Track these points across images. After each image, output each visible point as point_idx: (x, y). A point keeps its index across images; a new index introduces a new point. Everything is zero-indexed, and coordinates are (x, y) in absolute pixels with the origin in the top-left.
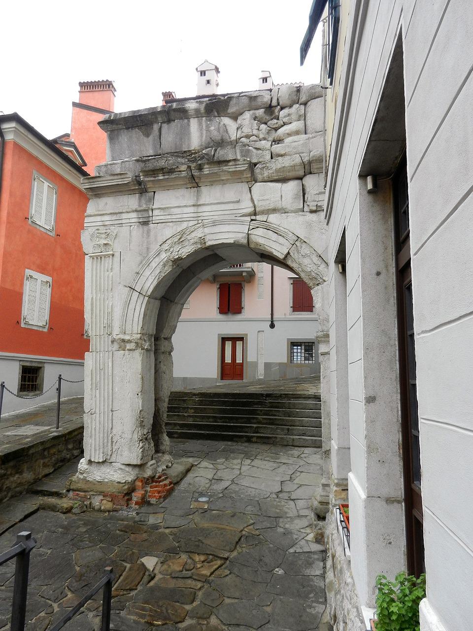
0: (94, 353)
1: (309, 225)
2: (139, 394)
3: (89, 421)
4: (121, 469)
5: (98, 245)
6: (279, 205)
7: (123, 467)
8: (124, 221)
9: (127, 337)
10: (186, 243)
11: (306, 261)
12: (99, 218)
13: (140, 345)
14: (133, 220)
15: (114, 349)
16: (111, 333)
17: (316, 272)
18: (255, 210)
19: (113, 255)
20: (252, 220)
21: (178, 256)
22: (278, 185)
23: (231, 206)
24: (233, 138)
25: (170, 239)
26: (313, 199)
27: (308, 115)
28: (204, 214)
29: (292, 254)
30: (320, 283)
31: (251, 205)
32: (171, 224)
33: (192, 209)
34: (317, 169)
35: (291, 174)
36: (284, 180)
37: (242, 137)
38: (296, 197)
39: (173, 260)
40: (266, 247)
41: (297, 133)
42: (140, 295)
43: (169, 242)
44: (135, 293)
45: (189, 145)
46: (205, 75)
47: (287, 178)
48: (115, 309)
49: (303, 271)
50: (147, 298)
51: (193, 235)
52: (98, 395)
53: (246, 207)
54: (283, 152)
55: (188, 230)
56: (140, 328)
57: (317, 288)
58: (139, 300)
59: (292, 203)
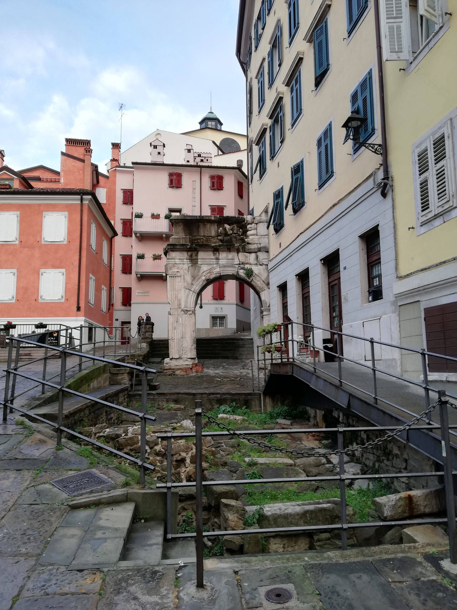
3: (171, 343)
9: (189, 309)
11: (258, 283)
23: (230, 261)
27: (258, 228)
33: (215, 260)
41: (254, 235)
46: (156, 148)
48: (182, 298)
51: (215, 270)
53: (236, 262)
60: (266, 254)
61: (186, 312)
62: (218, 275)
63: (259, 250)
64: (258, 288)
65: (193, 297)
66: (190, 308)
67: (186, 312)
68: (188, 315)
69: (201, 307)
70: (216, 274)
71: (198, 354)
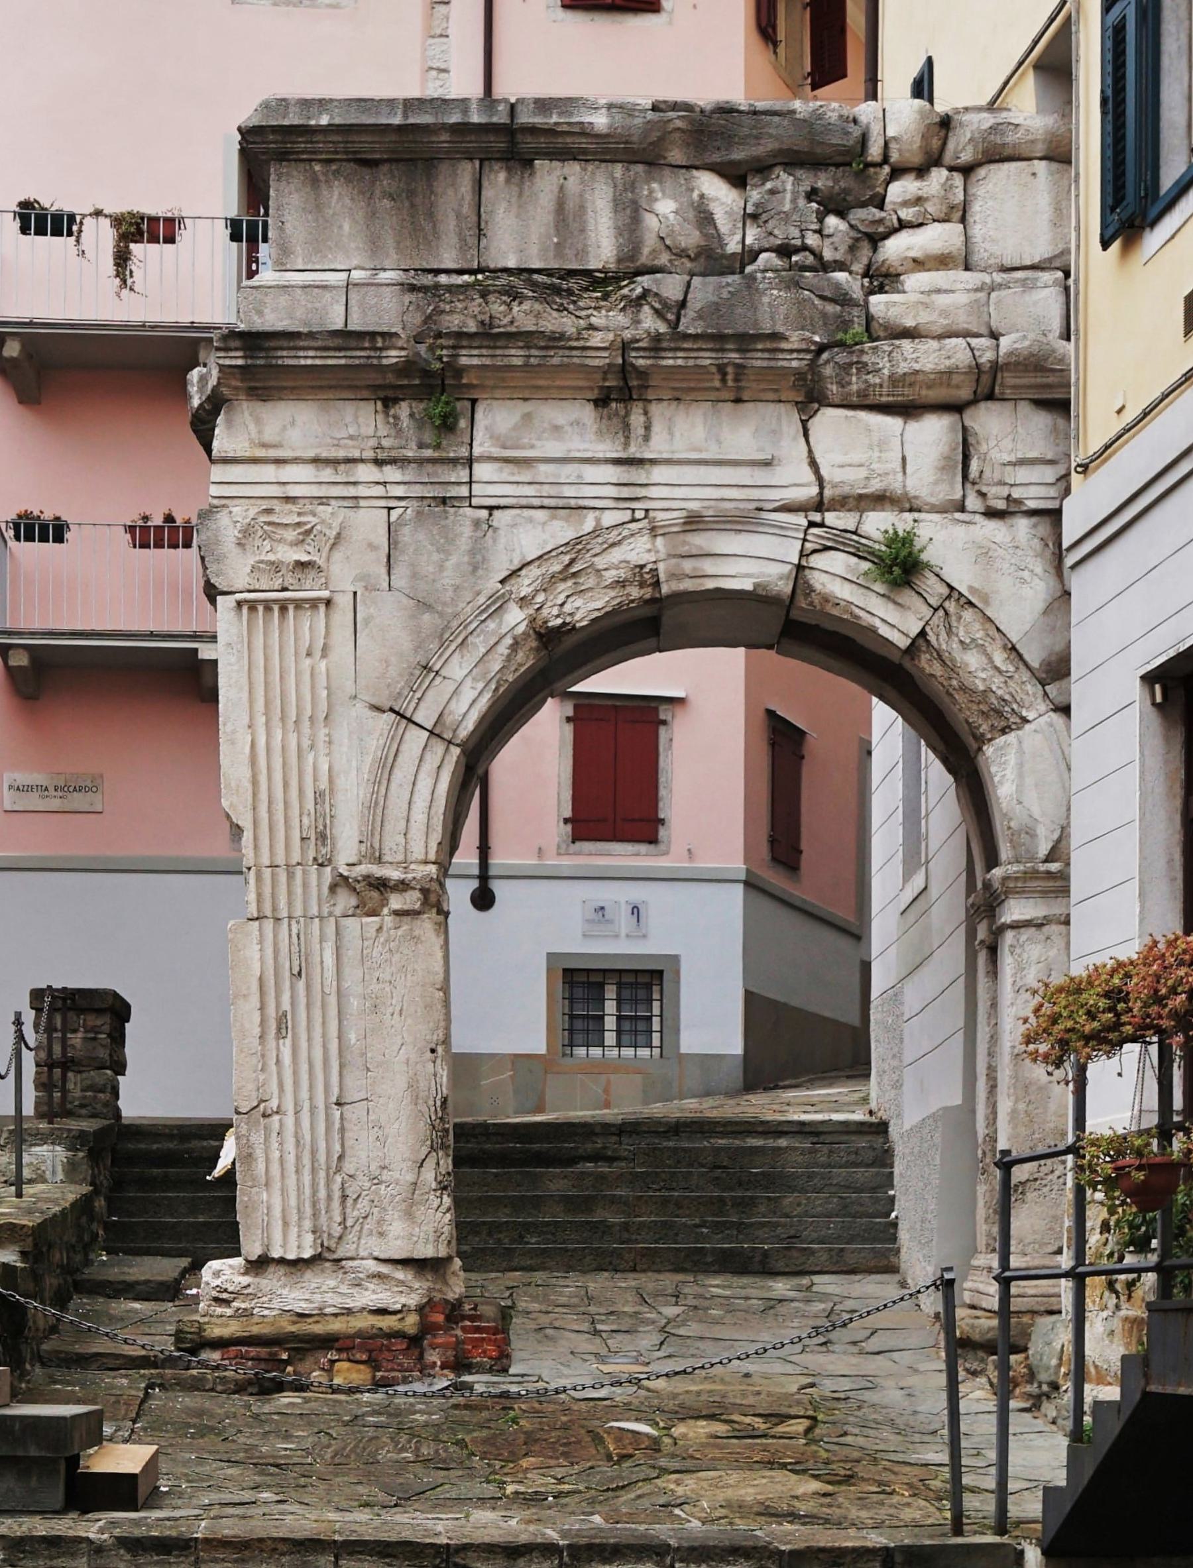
0: (269, 925)
1: (984, 555)
2: (440, 1049)
4: (379, 1276)
5: (273, 563)
6: (895, 484)
7: (385, 1269)
8: (362, 491)
9: (395, 874)
10: (589, 581)
11: (972, 660)
12: (269, 472)
13: (433, 898)
14: (399, 491)
15: (338, 911)
16: (330, 860)
17: (1000, 692)
18: (821, 493)
19: (328, 603)
20: (812, 524)
21: (559, 621)
22: (892, 424)
24: (733, 246)
25: (537, 564)
26: (997, 476)
28: (654, 492)
29: (932, 637)
30: (1009, 727)
31: (811, 477)
32: (540, 515)
34: (1014, 387)
35: (932, 395)
36: (908, 410)
37: (766, 250)
38: (945, 467)
39: (543, 631)
40: (857, 611)
41: (942, 262)
42: (434, 740)
43: (534, 572)
44: (413, 731)
45: (582, 253)
47: (918, 402)
48: (341, 782)
49: (963, 688)
50: (456, 751)
51: (616, 555)
52: (287, 1059)
54: (909, 323)
55: (600, 540)
56: (433, 847)
57: (1001, 740)
58: (428, 756)
59: (936, 483)
60: (1042, 420)
61: (373, 891)
62: (635, 592)
63: (987, 385)
64: (964, 712)
65: (427, 780)
66: (405, 864)
67: (373, 891)
68: (389, 921)
69: (483, 899)
70: (621, 583)
71: (463, 1230)
